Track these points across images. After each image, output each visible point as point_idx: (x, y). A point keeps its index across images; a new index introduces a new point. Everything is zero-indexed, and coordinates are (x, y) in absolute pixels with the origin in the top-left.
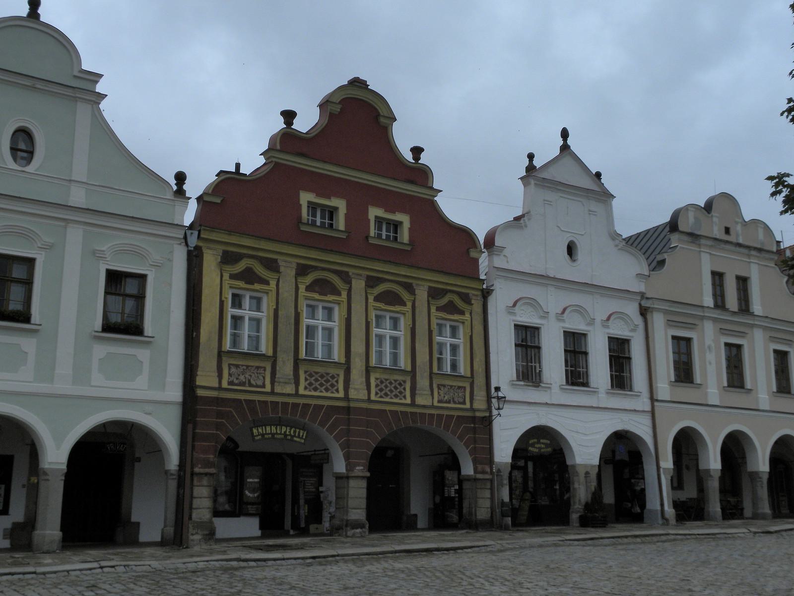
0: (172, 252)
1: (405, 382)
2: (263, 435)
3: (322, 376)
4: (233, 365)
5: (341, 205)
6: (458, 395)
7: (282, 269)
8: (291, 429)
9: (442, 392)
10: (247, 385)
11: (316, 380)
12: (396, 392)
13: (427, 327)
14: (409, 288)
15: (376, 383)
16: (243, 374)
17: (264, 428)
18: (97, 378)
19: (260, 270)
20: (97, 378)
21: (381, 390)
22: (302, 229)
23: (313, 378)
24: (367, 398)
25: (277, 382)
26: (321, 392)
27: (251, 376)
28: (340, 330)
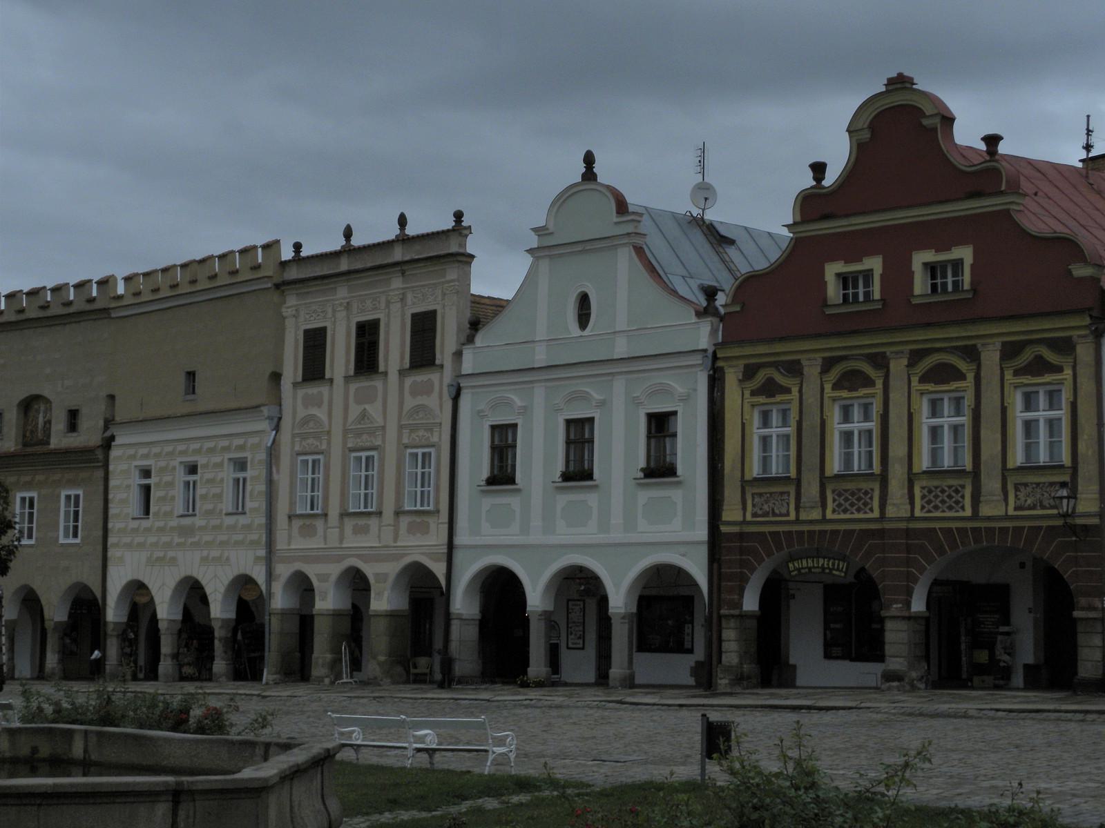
0: (696, 381)
1: (963, 487)
2: (799, 570)
3: (853, 494)
4: (757, 494)
5: (875, 264)
6: (1050, 495)
8: (829, 561)
9: (1021, 495)
10: (771, 515)
11: (846, 500)
13: (998, 404)
14: (971, 354)
15: (921, 494)
16: (766, 503)
21: (929, 502)
22: (827, 313)
23: (843, 498)
24: (909, 515)
26: (852, 513)
27: (774, 504)
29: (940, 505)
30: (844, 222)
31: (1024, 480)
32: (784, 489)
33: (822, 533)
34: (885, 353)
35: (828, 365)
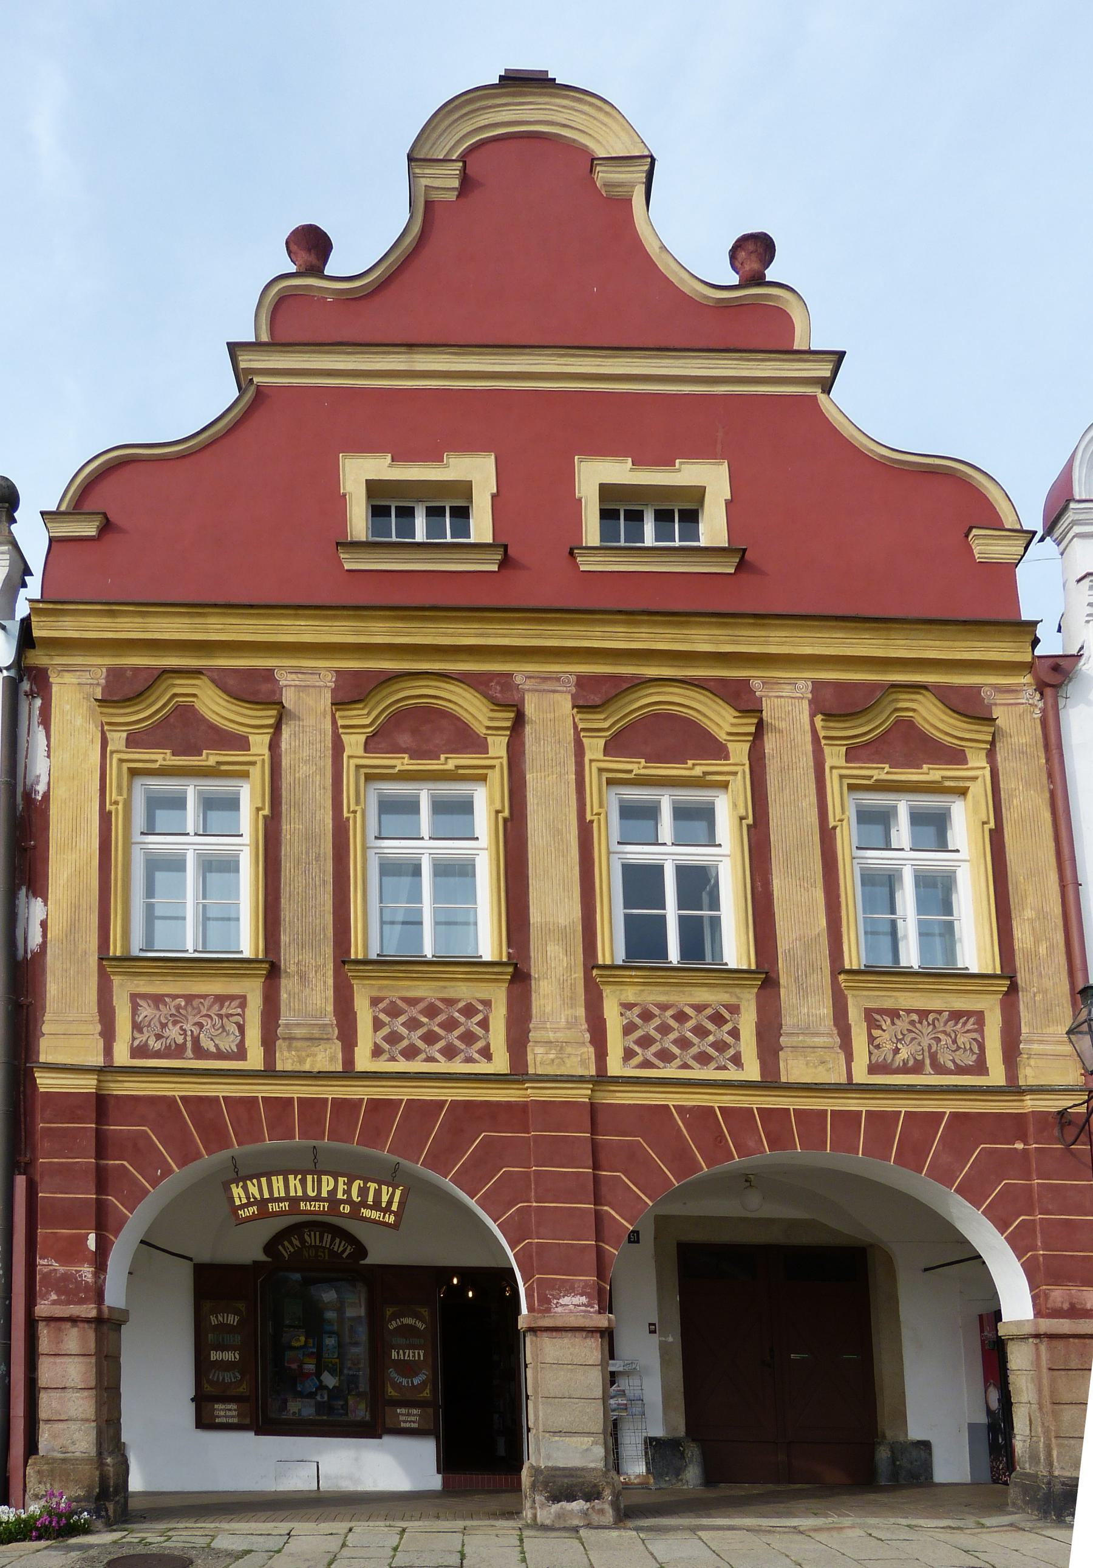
1: (734, 1009)
3: (432, 1011)
4: (144, 996)
6: (954, 1042)
9: (885, 1037)
10: (189, 1053)
11: (413, 1024)
16: (175, 1023)
21: (646, 1042)
23: (402, 1019)
25: (284, 1039)
26: (430, 1059)
27: (201, 1025)
29: (676, 1050)
31: (888, 1004)
33: (345, 1107)
34: (509, 675)
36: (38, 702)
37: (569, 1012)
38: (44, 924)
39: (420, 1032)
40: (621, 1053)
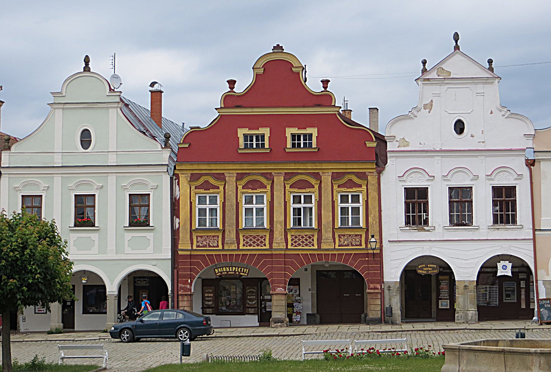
1: (313, 236)
2: (221, 272)
3: (254, 238)
4: (199, 236)
5: (266, 131)
6: (356, 240)
7: (227, 179)
10: (208, 246)
11: (251, 240)
12: (306, 242)
14: (317, 176)
16: (205, 241)
17: (222, 268)
18: (128, 250)
19: (212, 181)
20: (128, 250)
21: (296, 242)
22: (239, 152)
23: (249, 239)
26: (254, 246)
27: (210, 241)
28: (267, 209)
29: (301, 243)
30: (250, 110)
31: (343, 234)
32: (216, 235)
35: (240, 177)
36: (177, 181)
37: (281, 237)
38: (179, 223)
39: (252, 241)
40: (291, 244)
